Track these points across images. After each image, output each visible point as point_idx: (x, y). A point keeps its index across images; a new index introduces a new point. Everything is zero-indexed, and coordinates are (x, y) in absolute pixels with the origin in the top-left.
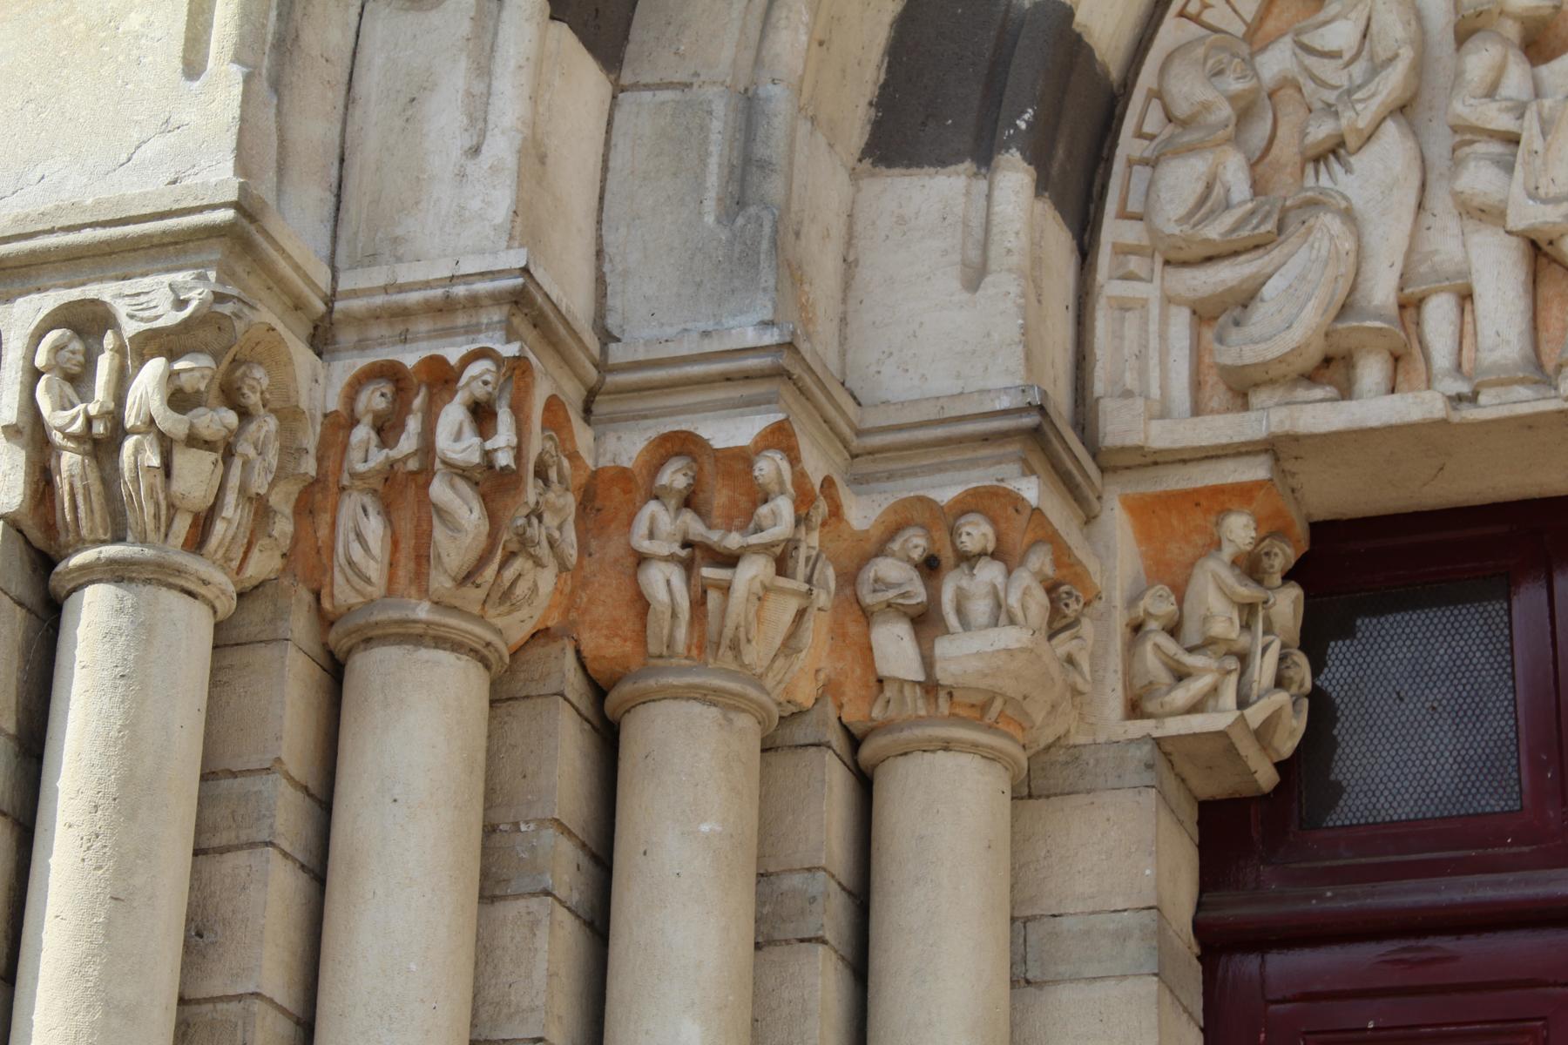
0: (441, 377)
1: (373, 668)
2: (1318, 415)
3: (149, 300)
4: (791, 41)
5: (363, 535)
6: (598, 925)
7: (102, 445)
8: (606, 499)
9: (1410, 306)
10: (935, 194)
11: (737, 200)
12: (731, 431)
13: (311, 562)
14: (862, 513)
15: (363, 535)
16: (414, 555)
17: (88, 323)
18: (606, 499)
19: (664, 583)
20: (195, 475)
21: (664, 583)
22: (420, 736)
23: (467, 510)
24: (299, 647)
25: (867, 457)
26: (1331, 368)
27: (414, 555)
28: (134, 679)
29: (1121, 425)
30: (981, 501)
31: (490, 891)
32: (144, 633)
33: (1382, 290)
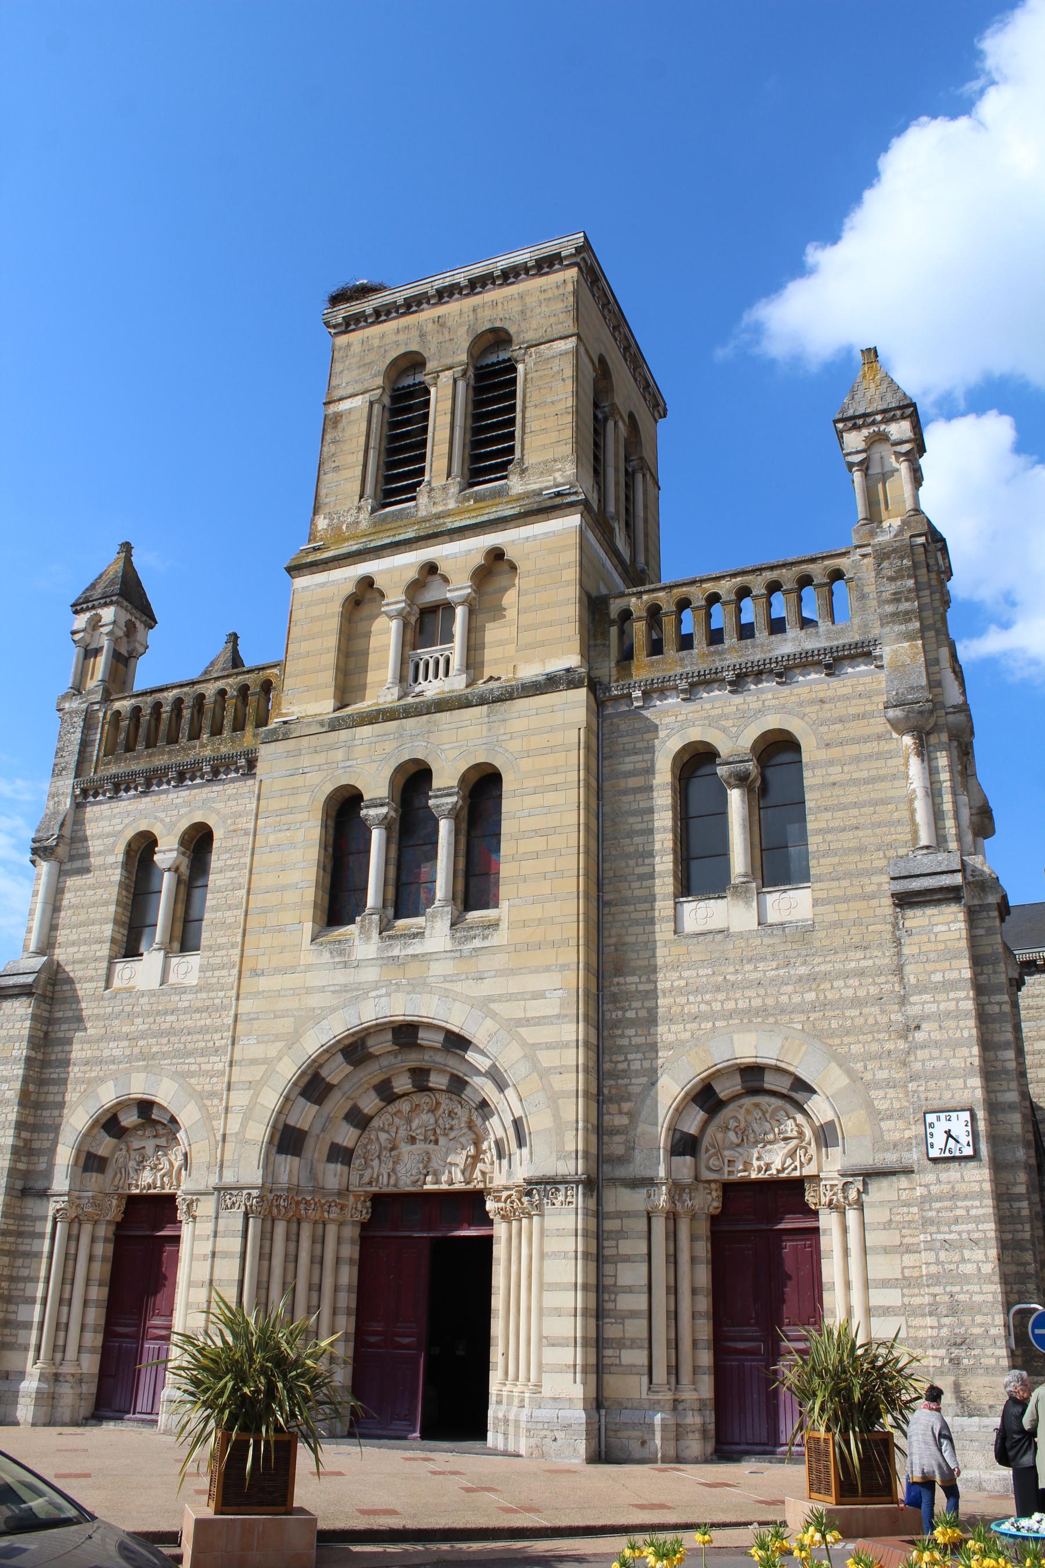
0: (281, 1196)
1: (276, 1222)
2: (368, 1189)
3: (255, 1193)
4: (316, 1156)
5: (275, 1211)
6: (298, 1242)
7: (251, 1206)
8: (298, 1203)
9: (378, 1176)
10: (332, 1166)
11: (311, 1172)
12: (308, 1198)
13: (271, 1212)
14: (323, 1201)
15: (275, 1211)
16: (279, 1211)
17: (249, 1194)
18: (298, 1203)
19: (303, 1212)
20: (259, 1209)
21: (303, 1212)
22: (280, 1228)
23: (283, 1210)
24: (269, 1220)
25: (324, 1196)
26: (370, 1183)
27: (279, 1211)
28: (255, 1227)
29: (351, 1188)
30: (334, 1201)
31: (287, 1240)
32: (255, 1222)
33: (375, 1176)
